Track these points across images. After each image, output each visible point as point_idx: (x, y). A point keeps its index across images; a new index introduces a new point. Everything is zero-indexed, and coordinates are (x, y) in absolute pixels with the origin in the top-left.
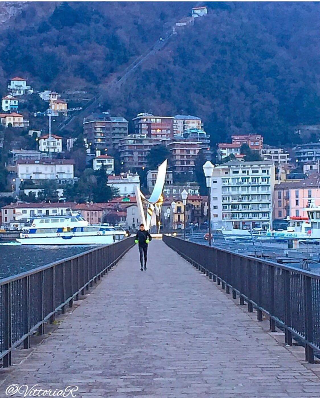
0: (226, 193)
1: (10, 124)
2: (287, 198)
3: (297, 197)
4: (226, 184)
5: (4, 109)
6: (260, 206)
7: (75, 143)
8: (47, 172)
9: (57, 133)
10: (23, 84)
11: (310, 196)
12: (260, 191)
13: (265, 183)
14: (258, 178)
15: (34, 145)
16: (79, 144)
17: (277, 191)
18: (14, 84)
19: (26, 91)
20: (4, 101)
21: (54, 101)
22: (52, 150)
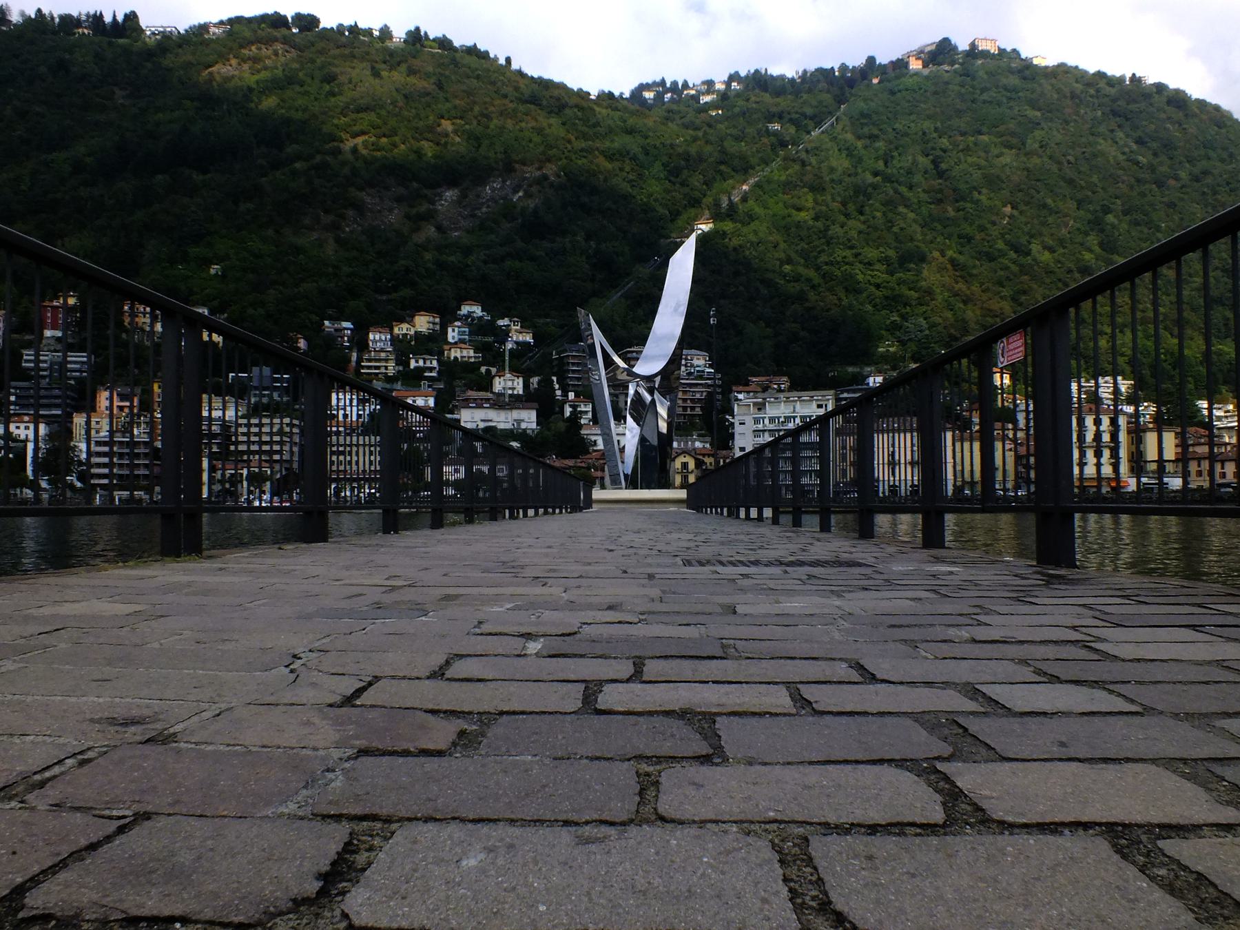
1: (456, 358)
5: (450, 340)
7: (539, 383)
8: (502, 420)
9: (515, 370)
10: (477, 311)
15: (486, 384)
16: (546, 384)
18: (465, 309)
20: (450, 330)
21: (516, 331)
22: (510, 392)
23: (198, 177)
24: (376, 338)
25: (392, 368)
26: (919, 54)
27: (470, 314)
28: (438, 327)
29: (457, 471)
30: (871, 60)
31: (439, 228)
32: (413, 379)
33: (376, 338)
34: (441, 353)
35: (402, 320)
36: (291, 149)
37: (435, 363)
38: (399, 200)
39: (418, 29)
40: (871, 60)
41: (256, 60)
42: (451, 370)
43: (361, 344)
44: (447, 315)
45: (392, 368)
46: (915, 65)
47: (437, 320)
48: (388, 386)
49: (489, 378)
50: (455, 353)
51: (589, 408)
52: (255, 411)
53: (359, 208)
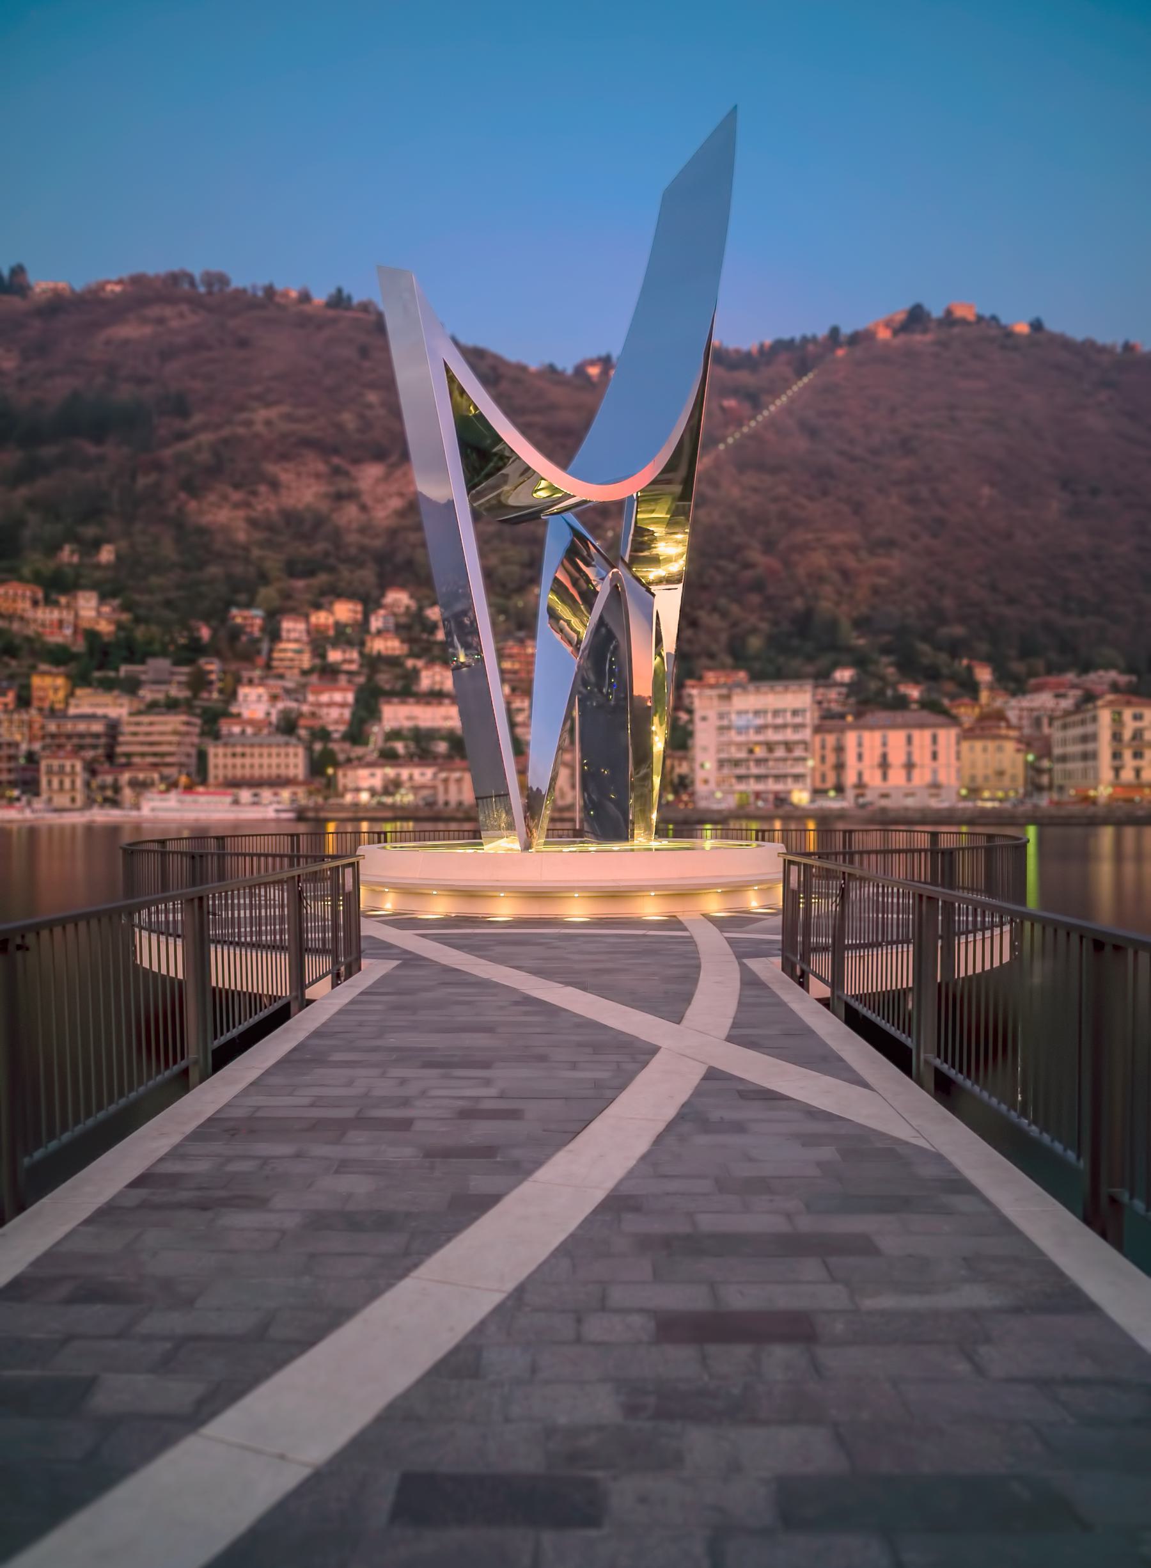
0: (724, 738)
2: (840, 749)
3: (860, 745)
4: (725, 722)
6: (789, 763)
11: (884, 744)
12: (789, 735)
13: (798, 720)
14: (785, 711)
17: (818, 739)
19: (408, 608)
23: (92, 450)
24: (292, 627)
25: (306, 661)
26: (888, 324)
27: (396, 603)
28: (359, 617)
29: (373, 775)
30: (835, 332)
31: (364, 508)
32: (329, 673)
33: (292, 627)
34: (362, 644)
35: (318, 607)
36: (197, 418)
37: (355, 655)
38: (318, 476)
39: (340, 291)
40: (835, 332)
41: (161, 321)
42: (373, 663)
43: (275, 635)
44: (370, 603)
45: (306, 661)
46: (884, 334)
47: (359, 608)
48: (303, 680)
49: (415, 674)
50: (379, 646)
51: (526, 704)
52: (152, 707)
53: (275, 485)
